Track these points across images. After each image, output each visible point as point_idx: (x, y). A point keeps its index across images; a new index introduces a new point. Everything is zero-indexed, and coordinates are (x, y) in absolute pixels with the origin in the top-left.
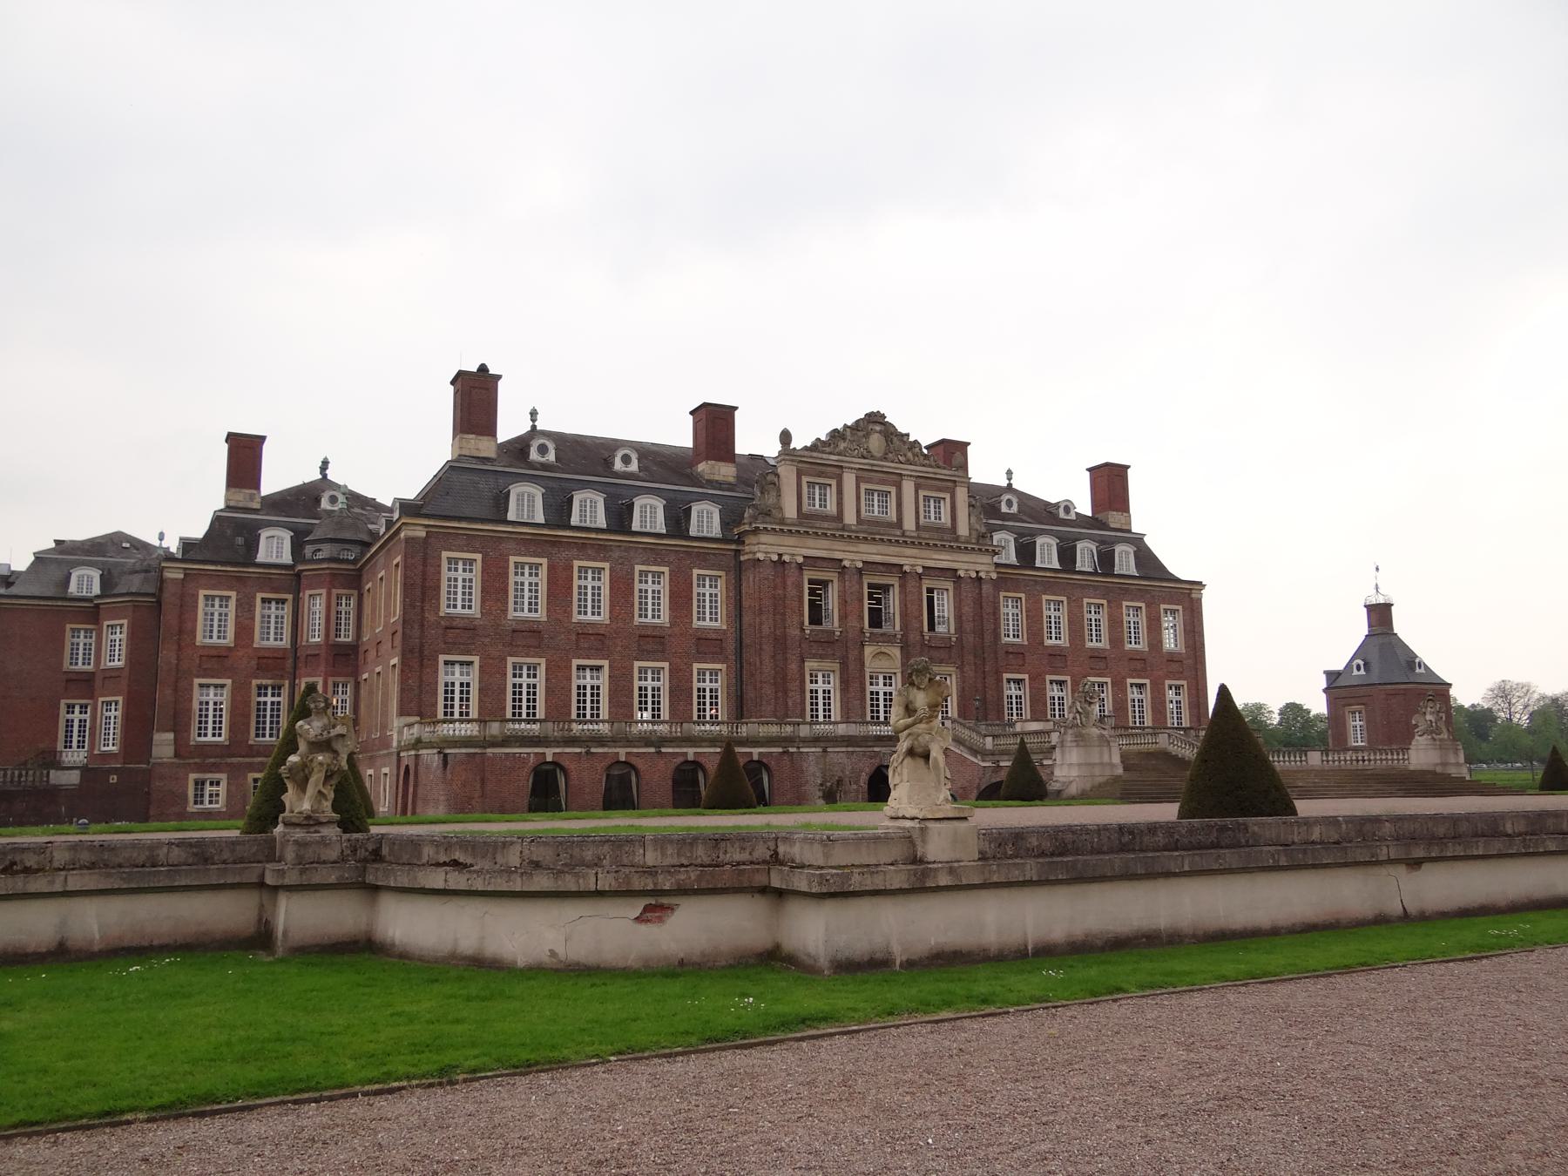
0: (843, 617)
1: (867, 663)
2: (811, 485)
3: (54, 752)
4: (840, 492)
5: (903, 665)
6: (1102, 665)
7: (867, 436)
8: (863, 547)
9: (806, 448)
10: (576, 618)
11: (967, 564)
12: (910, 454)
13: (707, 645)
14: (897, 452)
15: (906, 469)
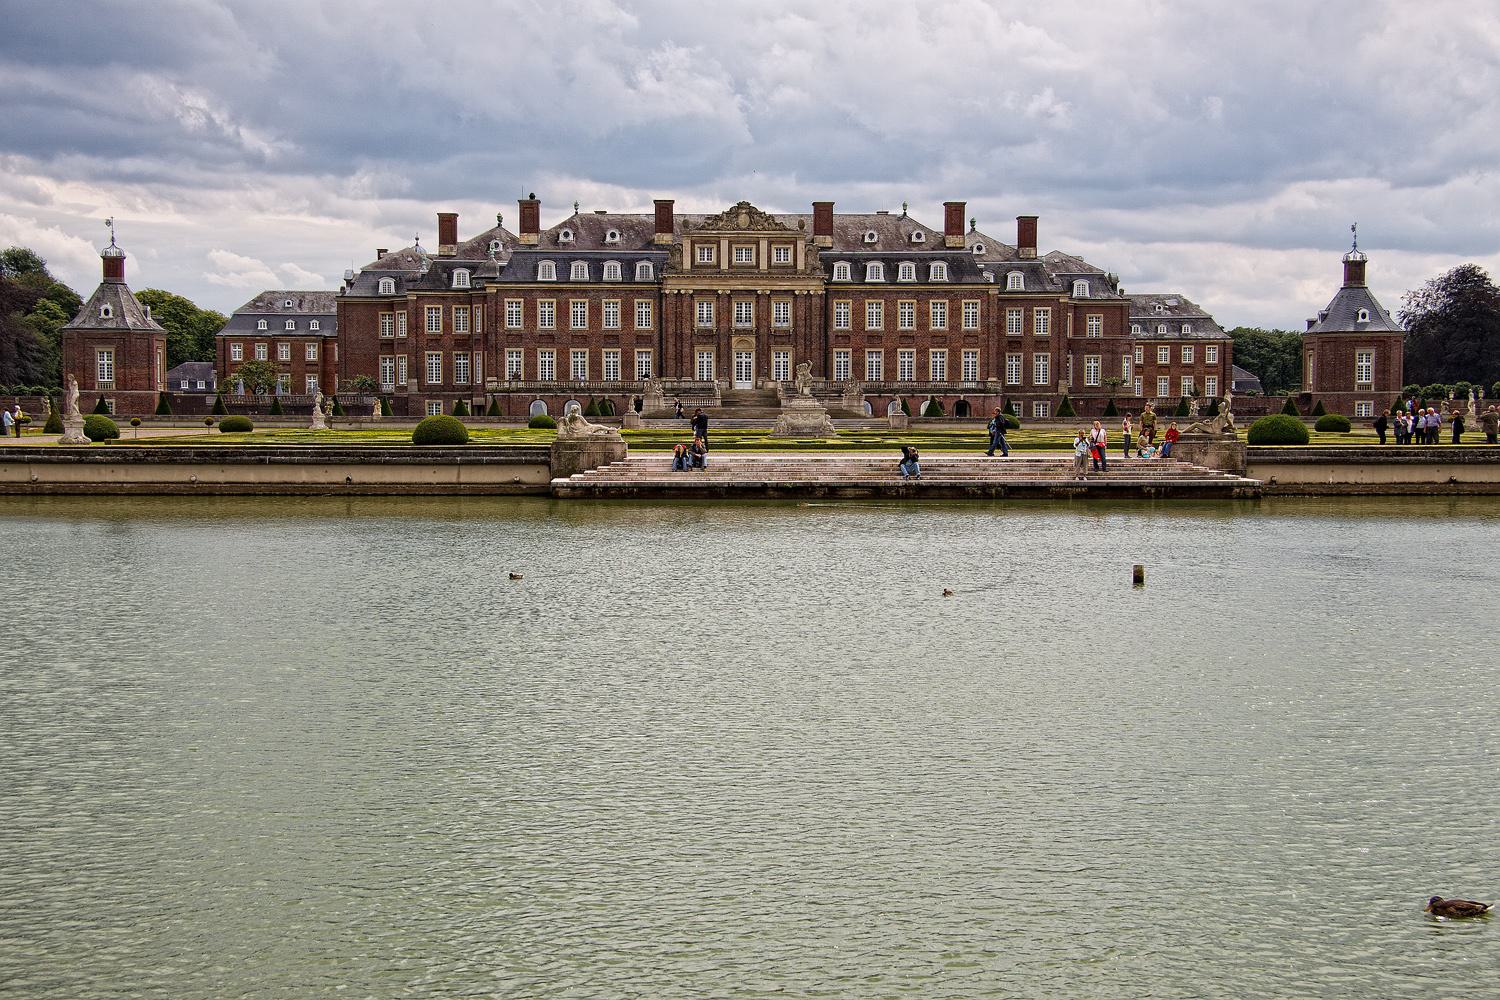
0: (718, 322)
2: (702, 249)
4: (719, 250)
6: (910, 341)
7: (737, 216)
8: (732, 282)
10: (572, 327)
11: (799, 287)
12: (766, 224)
13: (642, 339)
14: (757, 223)
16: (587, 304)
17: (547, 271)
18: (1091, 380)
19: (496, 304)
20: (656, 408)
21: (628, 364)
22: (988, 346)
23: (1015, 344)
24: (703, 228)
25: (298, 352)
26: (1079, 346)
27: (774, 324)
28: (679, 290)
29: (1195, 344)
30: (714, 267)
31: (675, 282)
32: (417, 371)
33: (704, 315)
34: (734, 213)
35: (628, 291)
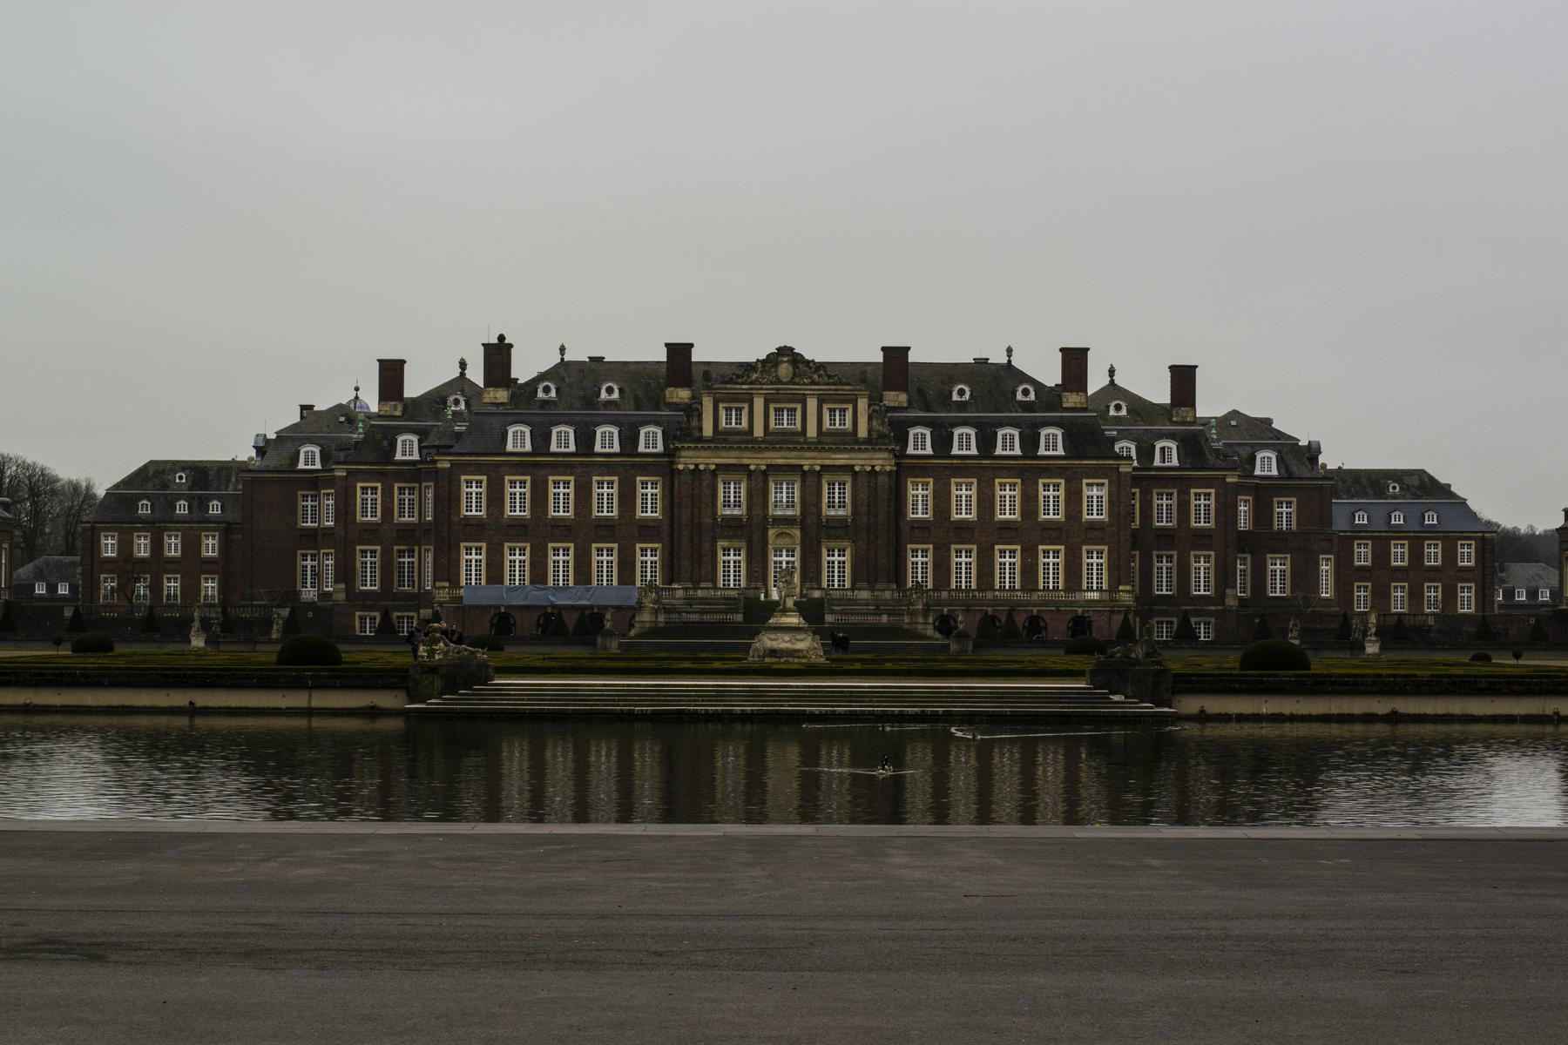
0: (749, 509)
2: (728, 410)
3: (297, 593)
11: (860, 461)
13: (647, 531)
14: (802, 376)
15: (809, 389)
17: (519, 438)
18: (1277, 589)
23: (1166, 538)
24: (731, 381)
25: (191, 546)
26: (1261, 542)
29: (1444, 540)
31: (690, 453)
32: (345, 572)
33: (731, 499)
35: (628, 466)
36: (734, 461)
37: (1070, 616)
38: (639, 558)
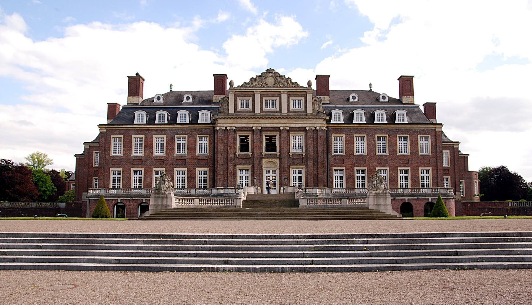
1: (263, 166)
2: (242, 100)
5: (280, 166)
6: (385, 162)
8: (262, 121)
9: (239, 86)
10: (155, 154)
11: (309, 125)
12: (286, 83)
13: (201, 162)
15: (283, 89)
16: (165, 138)
17: (140, 117)
19: (106, 140)
20: (164, 208)
21: (191, 179)
22: (437, 166)
27: (292, 150)
28: (226, 127)
30: (250, 112)
34: (263, 76)
36: (245, 125)
37: (425, 202)
38: (198, 176)
